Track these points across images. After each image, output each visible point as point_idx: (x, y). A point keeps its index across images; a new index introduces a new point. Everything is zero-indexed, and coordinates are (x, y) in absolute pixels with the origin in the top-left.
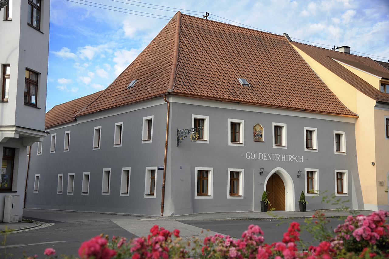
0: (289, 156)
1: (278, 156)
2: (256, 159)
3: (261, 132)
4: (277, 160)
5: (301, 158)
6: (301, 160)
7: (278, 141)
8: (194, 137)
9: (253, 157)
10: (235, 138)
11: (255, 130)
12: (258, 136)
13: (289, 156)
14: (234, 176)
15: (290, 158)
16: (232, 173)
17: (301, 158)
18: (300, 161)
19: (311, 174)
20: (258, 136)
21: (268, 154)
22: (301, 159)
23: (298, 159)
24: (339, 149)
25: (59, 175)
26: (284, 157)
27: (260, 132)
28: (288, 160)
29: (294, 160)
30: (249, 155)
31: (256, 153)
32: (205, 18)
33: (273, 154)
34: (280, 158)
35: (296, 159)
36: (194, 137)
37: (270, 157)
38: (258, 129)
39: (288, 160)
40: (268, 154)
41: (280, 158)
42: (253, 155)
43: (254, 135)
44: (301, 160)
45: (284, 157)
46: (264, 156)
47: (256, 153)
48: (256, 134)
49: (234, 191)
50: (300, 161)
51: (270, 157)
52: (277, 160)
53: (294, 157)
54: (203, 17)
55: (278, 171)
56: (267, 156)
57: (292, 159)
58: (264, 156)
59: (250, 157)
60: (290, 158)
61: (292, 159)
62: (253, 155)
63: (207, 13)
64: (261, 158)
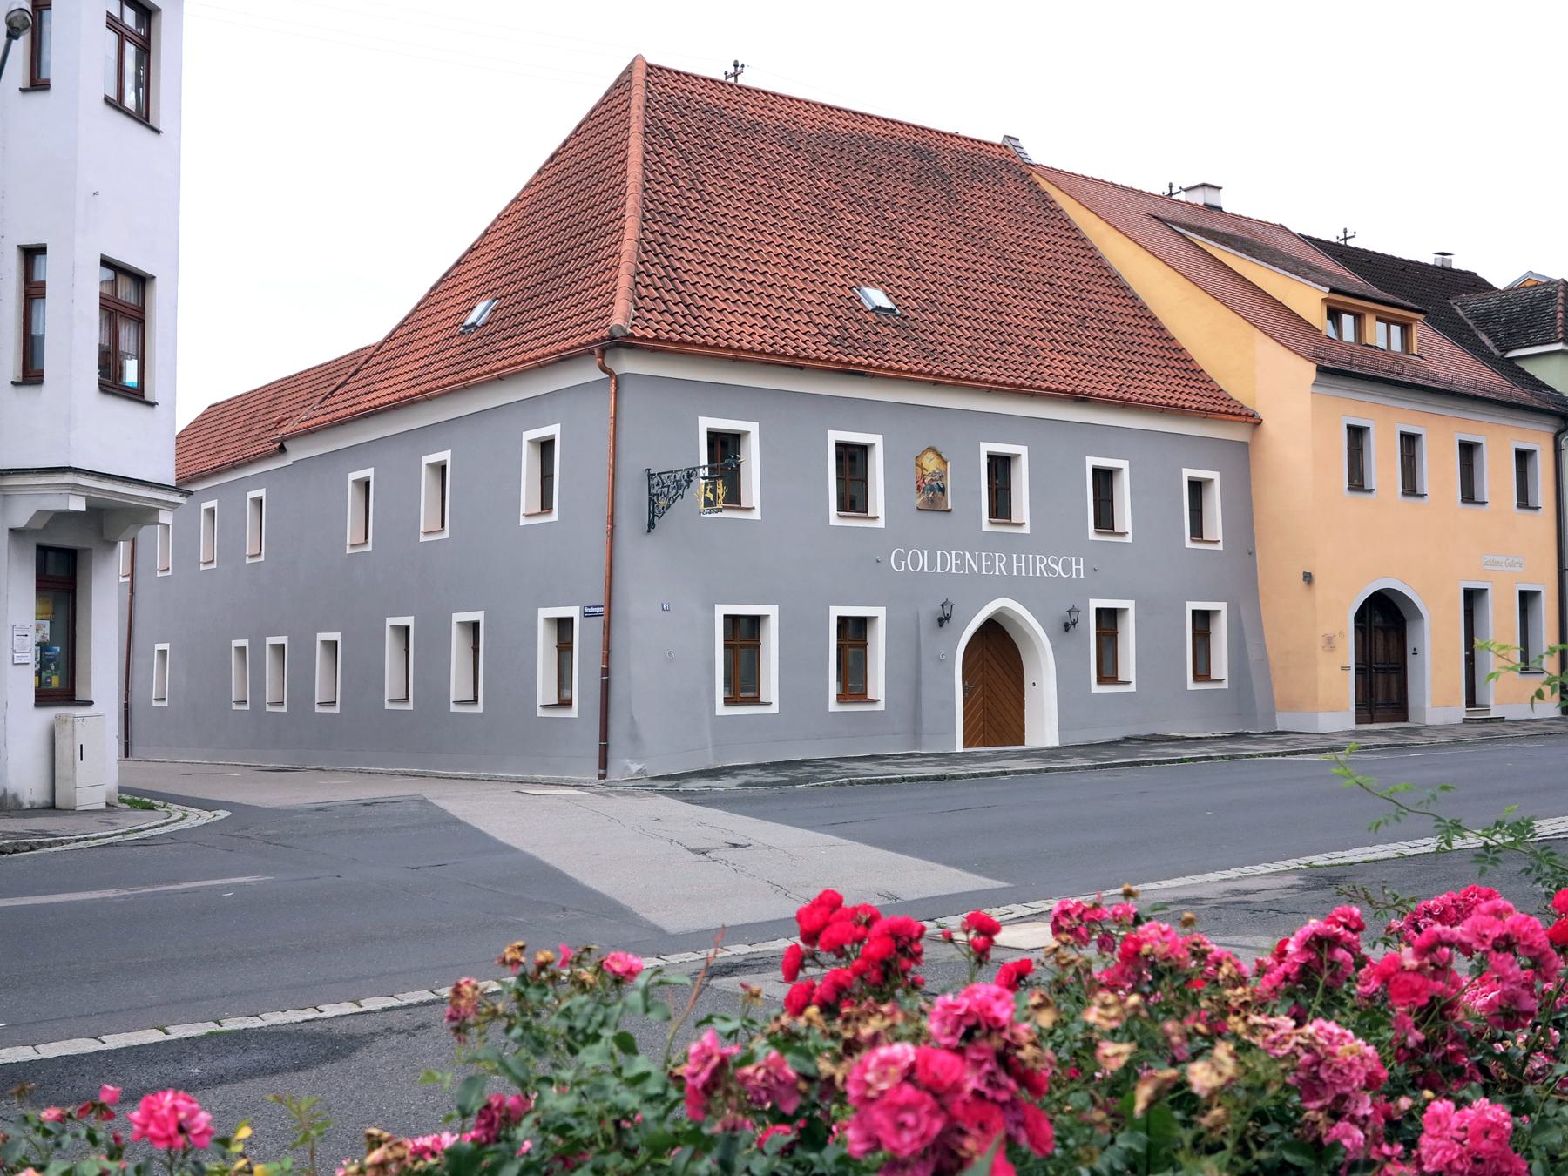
1: (1001, 560)
5: (1078, 563)
6: (1078, 571)
7: (1000, 506)
9: (915, 565)
10: (853, 499)
12: (932, 489)
14: (854, 632)
15: (1039, 565)
17: (1078, 563)
19: (1108, 620)
20: (932, 489)
22: (1079, 568)
23: (1067, 567)
24: (1197, 532)
26: (1019, 561)
29: (1054, 571)
30: (900, 558)
35: (1059, 569)
37: (975, 563)
38: (931, 463)
44: (1078, 571)
45: (1019, 561)
46: (952, 561)
49: (853, 682)
51: (975, 563)
53: (1053, 561)
55: (1000, 613)
57: (1047, 567)
58: (952, 561)
60: (1039, 565)
61: (1047, 567)
64: (943, 566)
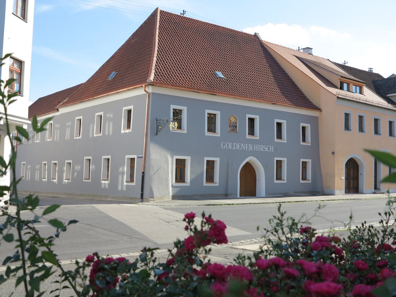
0: (261, 146)
1: (251, 146)
2: (231, 148)
3: (236, 123)
4: (250, 150)
5: (272, 148)
8: (174, 126)
9: (228, 147)
10: (212, 129)
11: (231, 121)
12: (233, 126)
13: (261, 146)
15: (261, 148)
16: (208, 161)
17: (272, 148)
18: (271, 151)
20: (233, 126)
21: (242, 144)
22: (272, 149)
24: (304, 140)
25: (23, 163)
26: (256, 147)
27: (235, 123)
28: (260, 150)
29: (265, 150)
31: (231, 143)
32: (182, 15)
33: (246, 144)
34: (253, 148)
35: (267, 149)
36: (174, 126)
37: (244, 147)
39: (260, 150)
40: (242, 144)
41: (253, 148)
42: (228, 145)
43: (229, 126)
45: (256, 147)
46: (238, 146)
47: (231, 143)
48: (231, 124)
50: (271, 151)
51: (244, 147)
52: (250, 150)
54: (180, 15)
56: (241, 145)
57: (263, 148)
58: (238, 146)
59: (225, 146)
60: (261, 148)
61: (263, 148)
62: (228, 145)
63: (184, 11)
64: (236, 147)
